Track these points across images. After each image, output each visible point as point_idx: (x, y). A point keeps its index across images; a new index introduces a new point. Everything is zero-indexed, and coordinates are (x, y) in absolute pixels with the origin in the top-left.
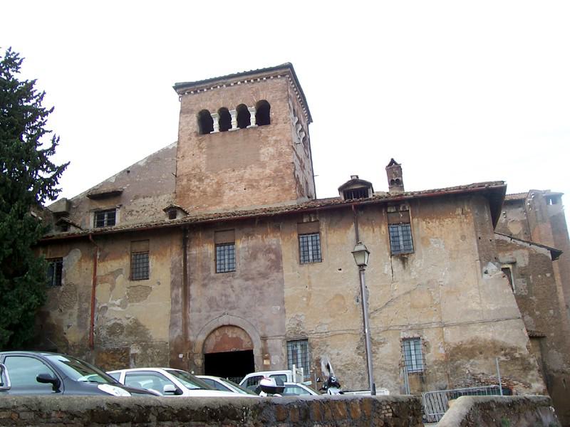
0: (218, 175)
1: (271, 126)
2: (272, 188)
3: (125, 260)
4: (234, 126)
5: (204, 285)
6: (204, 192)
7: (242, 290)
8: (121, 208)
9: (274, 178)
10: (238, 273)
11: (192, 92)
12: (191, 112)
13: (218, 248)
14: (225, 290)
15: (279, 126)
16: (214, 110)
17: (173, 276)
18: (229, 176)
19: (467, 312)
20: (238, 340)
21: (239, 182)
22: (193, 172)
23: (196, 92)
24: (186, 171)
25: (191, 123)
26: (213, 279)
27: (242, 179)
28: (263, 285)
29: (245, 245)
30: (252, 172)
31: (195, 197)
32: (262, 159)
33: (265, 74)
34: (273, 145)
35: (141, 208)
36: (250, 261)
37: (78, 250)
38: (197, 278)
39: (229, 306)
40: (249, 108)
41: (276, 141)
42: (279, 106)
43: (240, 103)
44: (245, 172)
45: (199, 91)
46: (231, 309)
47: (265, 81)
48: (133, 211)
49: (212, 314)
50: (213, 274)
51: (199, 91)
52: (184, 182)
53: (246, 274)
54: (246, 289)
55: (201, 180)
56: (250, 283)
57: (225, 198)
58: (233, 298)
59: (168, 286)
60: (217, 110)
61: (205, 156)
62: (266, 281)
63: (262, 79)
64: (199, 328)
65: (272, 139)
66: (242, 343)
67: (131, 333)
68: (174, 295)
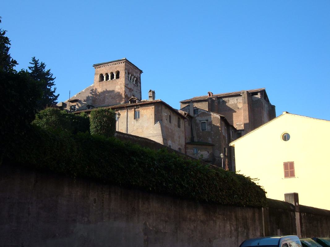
1: (119, 79)
6: (100, 100)
19: (149, 134)
23: (99, 68)
27: (110, 96)
34: (119, 85)
41: (120, 84)
43: (111, 71)
57: (106, 102)
65: (119, 83)
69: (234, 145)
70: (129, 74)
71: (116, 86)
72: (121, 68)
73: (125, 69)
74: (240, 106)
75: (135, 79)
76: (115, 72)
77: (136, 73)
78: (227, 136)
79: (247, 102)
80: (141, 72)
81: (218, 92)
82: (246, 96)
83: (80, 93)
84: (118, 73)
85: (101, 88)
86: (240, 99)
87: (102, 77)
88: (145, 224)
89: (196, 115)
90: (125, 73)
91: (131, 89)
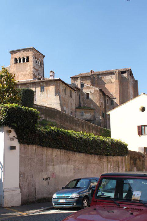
12: (13, 58)
18: (20, 73)
27: (22, 74)
30: (24, 73)
32: (27, 70)
57: (19, 78)
69: (110, 113)
70: (35, 58)
71: (26, 68)
72: (30, 54)
73: (33, 55)
74: (113, 81)
75: (40, 62)
77: (41, 57)
78: (103, 103)
79: (118, 79)
80: (44, 56)
81: (97, 70)
82: (118, 74)
84: (28, 58)
86: (113, 76)
87: (16, 60)
88: (74, 165)
89: (82, 88)
90: (33, 58)
91: (37, 69)
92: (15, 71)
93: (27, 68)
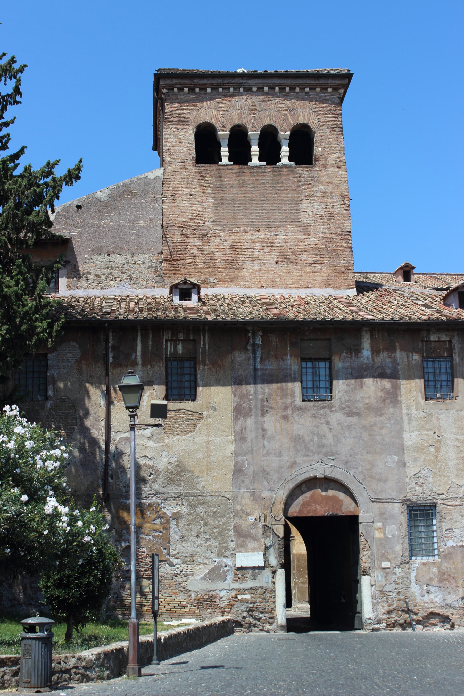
0: (234, 234)
1: (317, 168)
2: (319, 266)
3: (157, 369)
4: (255, 161)
5: (285, 418)
6: (211, 257)
7: (342, 429)
8: (69, 267)
9: (321, 252)
10: (336, 401)
11: (186, 90)
13: (304, 364)
14: (317, 427)
15: (331, 170)
16: (224, 127)
17: (236, 399)
20: (335, 499)
21: (267, 250)
22: (192, 224)
24: (181, 220)
25: (186, 142)
26: (300, 409)
28: (375, 425)
29: (348, 364)
31: (195, 264)
32: (303, 218)
33: (308, 81)
34: (320, 200)
35: (103, 272)
36: (355, 389)
37: (75, 344)
38: (274, 405)
39: (324, 450)
40: (281, 133)
41: (325, 194)
42: (328, 137)
43: (267, 122)
44: (276, 235)
45: (197, 90)
46: (326, 454)
47: (307, 93)
48: (90, 273)
49: (299, 459)
50: (298, 401)
51: (197, 90)
52: (177, 237)
53: (349, 407)
54: (349, 427)
55: (203, 237)
56: (354, 419)
57: (245, 273)
58: (329, 440)
59: (230, 415)
60: (229, 127)
61: (210, 200)
62: (378, 419)
63: (302, 89)
64: (280, 479)
66: (341, 506)
67: (170, 481)
68: (238, 428)
76: (285, 126)
83: (79, 207)
85: (208, 195)
92: (209, 217)
93: (305, 205)
